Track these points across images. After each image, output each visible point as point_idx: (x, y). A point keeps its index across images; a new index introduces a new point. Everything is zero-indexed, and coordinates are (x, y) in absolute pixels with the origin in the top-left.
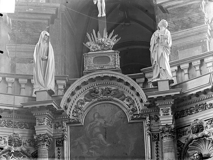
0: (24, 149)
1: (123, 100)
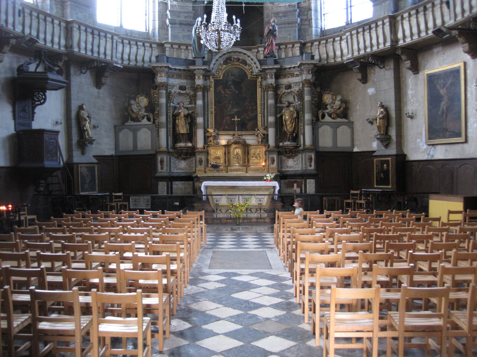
0: (188, 92)
1: (246, 65)
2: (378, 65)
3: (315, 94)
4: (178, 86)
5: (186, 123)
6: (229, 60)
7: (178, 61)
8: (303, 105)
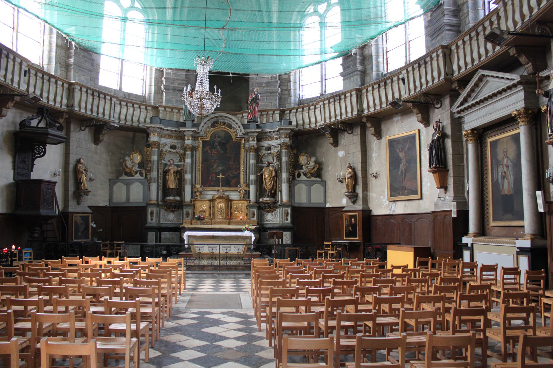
1: (231, 129)
2: (347, 131)
3: (292, 156)
4: (169, 145)
5: (175, 179)
7: (170, 123)
8: (281, 165)
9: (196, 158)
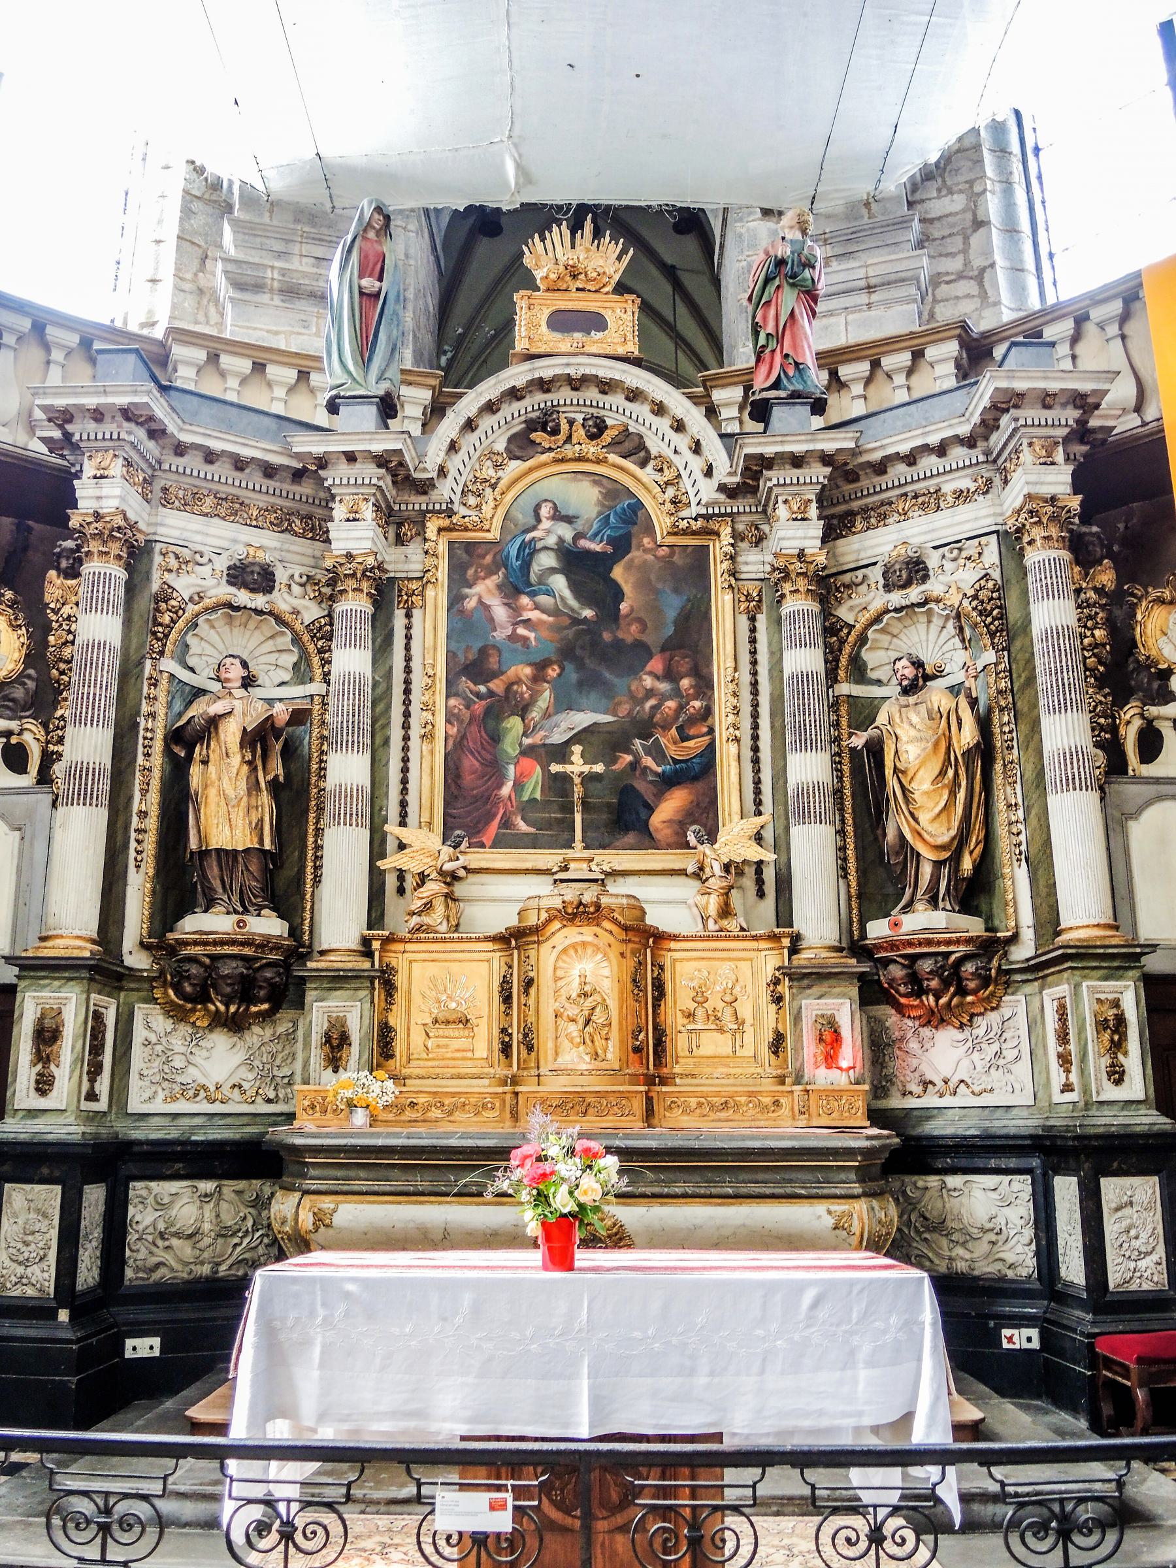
1: (643, 464)
4: (222, 564)
5: (254, 787)
6: (544, 430)
9: (408, 659)
